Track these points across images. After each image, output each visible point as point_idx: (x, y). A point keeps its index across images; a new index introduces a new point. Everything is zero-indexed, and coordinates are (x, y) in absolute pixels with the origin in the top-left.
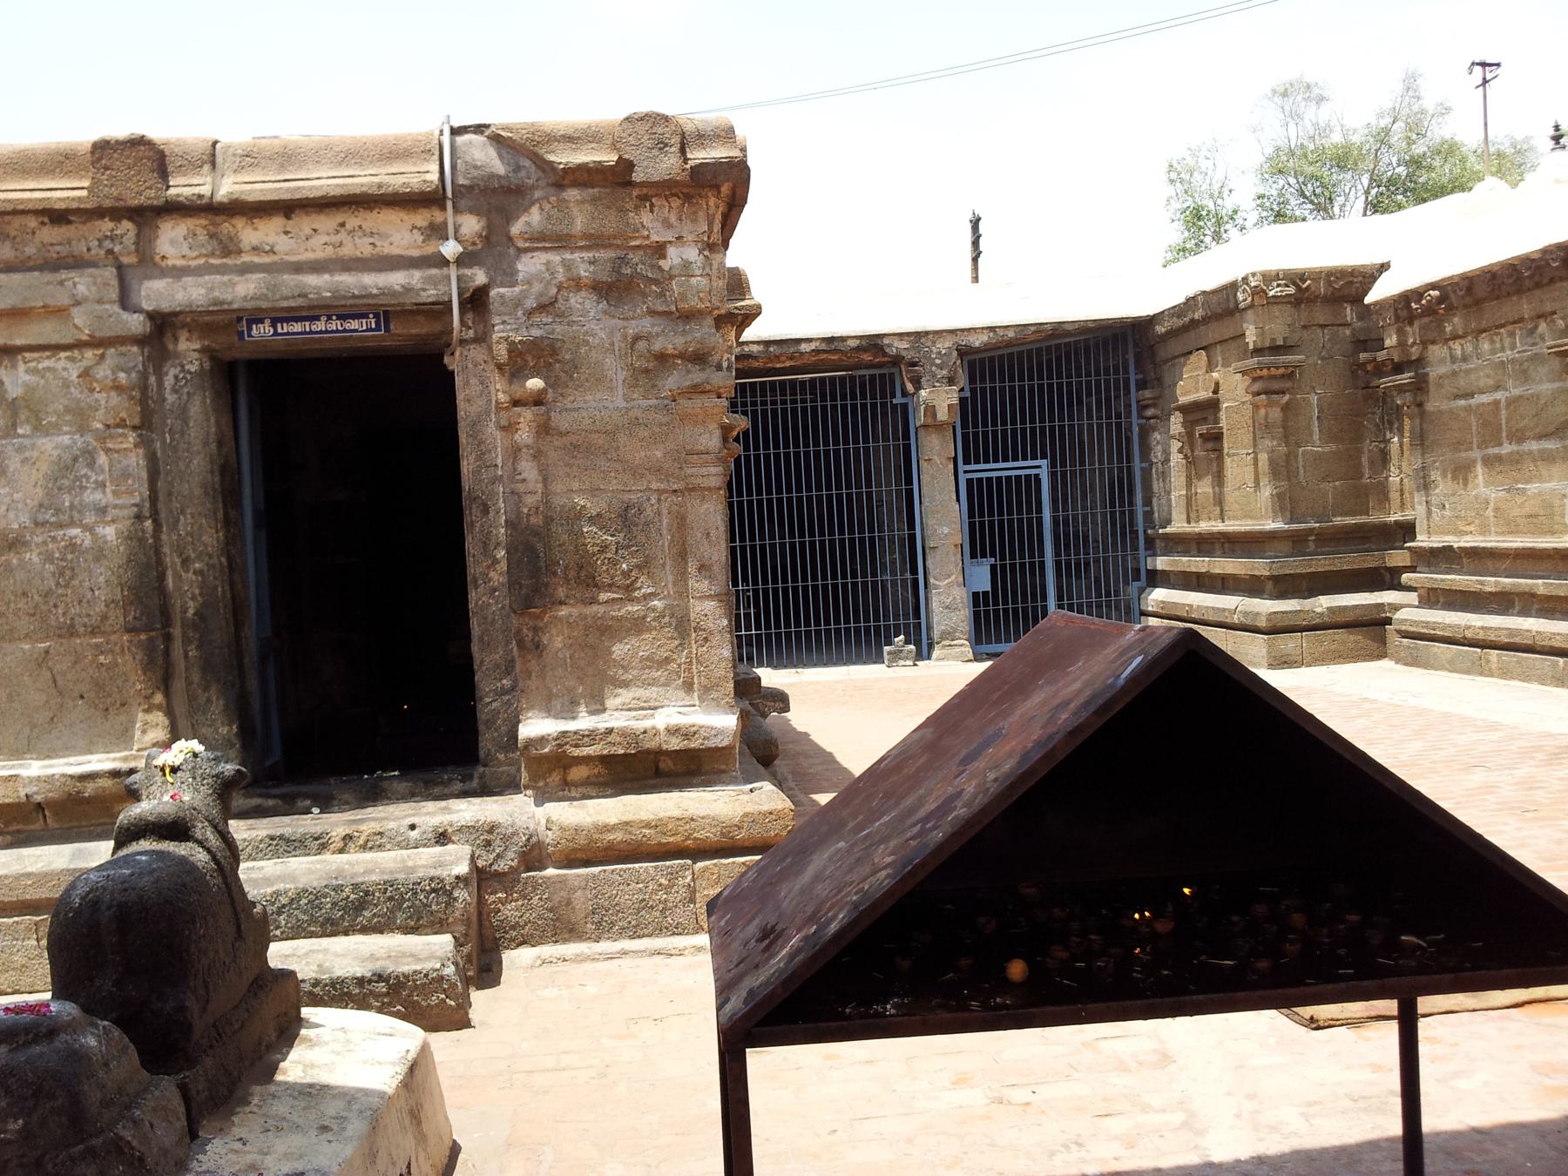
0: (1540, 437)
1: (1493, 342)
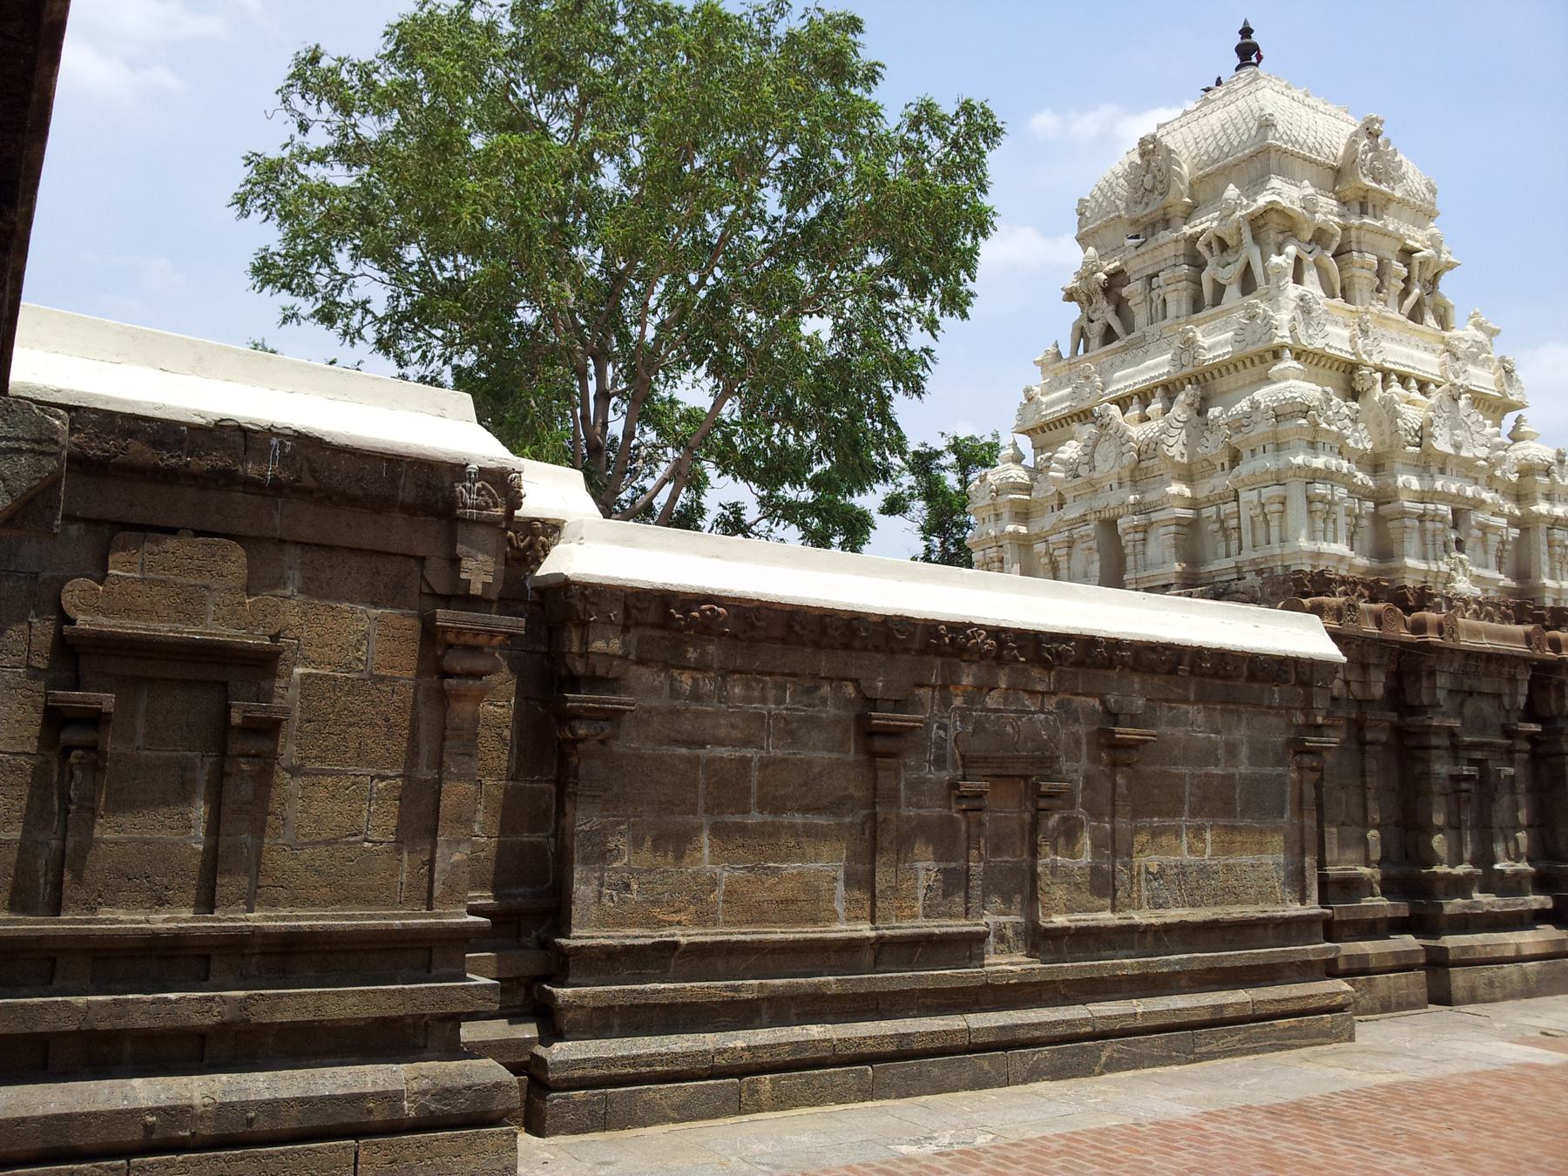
0: (805, 810)
1: (748, 687)
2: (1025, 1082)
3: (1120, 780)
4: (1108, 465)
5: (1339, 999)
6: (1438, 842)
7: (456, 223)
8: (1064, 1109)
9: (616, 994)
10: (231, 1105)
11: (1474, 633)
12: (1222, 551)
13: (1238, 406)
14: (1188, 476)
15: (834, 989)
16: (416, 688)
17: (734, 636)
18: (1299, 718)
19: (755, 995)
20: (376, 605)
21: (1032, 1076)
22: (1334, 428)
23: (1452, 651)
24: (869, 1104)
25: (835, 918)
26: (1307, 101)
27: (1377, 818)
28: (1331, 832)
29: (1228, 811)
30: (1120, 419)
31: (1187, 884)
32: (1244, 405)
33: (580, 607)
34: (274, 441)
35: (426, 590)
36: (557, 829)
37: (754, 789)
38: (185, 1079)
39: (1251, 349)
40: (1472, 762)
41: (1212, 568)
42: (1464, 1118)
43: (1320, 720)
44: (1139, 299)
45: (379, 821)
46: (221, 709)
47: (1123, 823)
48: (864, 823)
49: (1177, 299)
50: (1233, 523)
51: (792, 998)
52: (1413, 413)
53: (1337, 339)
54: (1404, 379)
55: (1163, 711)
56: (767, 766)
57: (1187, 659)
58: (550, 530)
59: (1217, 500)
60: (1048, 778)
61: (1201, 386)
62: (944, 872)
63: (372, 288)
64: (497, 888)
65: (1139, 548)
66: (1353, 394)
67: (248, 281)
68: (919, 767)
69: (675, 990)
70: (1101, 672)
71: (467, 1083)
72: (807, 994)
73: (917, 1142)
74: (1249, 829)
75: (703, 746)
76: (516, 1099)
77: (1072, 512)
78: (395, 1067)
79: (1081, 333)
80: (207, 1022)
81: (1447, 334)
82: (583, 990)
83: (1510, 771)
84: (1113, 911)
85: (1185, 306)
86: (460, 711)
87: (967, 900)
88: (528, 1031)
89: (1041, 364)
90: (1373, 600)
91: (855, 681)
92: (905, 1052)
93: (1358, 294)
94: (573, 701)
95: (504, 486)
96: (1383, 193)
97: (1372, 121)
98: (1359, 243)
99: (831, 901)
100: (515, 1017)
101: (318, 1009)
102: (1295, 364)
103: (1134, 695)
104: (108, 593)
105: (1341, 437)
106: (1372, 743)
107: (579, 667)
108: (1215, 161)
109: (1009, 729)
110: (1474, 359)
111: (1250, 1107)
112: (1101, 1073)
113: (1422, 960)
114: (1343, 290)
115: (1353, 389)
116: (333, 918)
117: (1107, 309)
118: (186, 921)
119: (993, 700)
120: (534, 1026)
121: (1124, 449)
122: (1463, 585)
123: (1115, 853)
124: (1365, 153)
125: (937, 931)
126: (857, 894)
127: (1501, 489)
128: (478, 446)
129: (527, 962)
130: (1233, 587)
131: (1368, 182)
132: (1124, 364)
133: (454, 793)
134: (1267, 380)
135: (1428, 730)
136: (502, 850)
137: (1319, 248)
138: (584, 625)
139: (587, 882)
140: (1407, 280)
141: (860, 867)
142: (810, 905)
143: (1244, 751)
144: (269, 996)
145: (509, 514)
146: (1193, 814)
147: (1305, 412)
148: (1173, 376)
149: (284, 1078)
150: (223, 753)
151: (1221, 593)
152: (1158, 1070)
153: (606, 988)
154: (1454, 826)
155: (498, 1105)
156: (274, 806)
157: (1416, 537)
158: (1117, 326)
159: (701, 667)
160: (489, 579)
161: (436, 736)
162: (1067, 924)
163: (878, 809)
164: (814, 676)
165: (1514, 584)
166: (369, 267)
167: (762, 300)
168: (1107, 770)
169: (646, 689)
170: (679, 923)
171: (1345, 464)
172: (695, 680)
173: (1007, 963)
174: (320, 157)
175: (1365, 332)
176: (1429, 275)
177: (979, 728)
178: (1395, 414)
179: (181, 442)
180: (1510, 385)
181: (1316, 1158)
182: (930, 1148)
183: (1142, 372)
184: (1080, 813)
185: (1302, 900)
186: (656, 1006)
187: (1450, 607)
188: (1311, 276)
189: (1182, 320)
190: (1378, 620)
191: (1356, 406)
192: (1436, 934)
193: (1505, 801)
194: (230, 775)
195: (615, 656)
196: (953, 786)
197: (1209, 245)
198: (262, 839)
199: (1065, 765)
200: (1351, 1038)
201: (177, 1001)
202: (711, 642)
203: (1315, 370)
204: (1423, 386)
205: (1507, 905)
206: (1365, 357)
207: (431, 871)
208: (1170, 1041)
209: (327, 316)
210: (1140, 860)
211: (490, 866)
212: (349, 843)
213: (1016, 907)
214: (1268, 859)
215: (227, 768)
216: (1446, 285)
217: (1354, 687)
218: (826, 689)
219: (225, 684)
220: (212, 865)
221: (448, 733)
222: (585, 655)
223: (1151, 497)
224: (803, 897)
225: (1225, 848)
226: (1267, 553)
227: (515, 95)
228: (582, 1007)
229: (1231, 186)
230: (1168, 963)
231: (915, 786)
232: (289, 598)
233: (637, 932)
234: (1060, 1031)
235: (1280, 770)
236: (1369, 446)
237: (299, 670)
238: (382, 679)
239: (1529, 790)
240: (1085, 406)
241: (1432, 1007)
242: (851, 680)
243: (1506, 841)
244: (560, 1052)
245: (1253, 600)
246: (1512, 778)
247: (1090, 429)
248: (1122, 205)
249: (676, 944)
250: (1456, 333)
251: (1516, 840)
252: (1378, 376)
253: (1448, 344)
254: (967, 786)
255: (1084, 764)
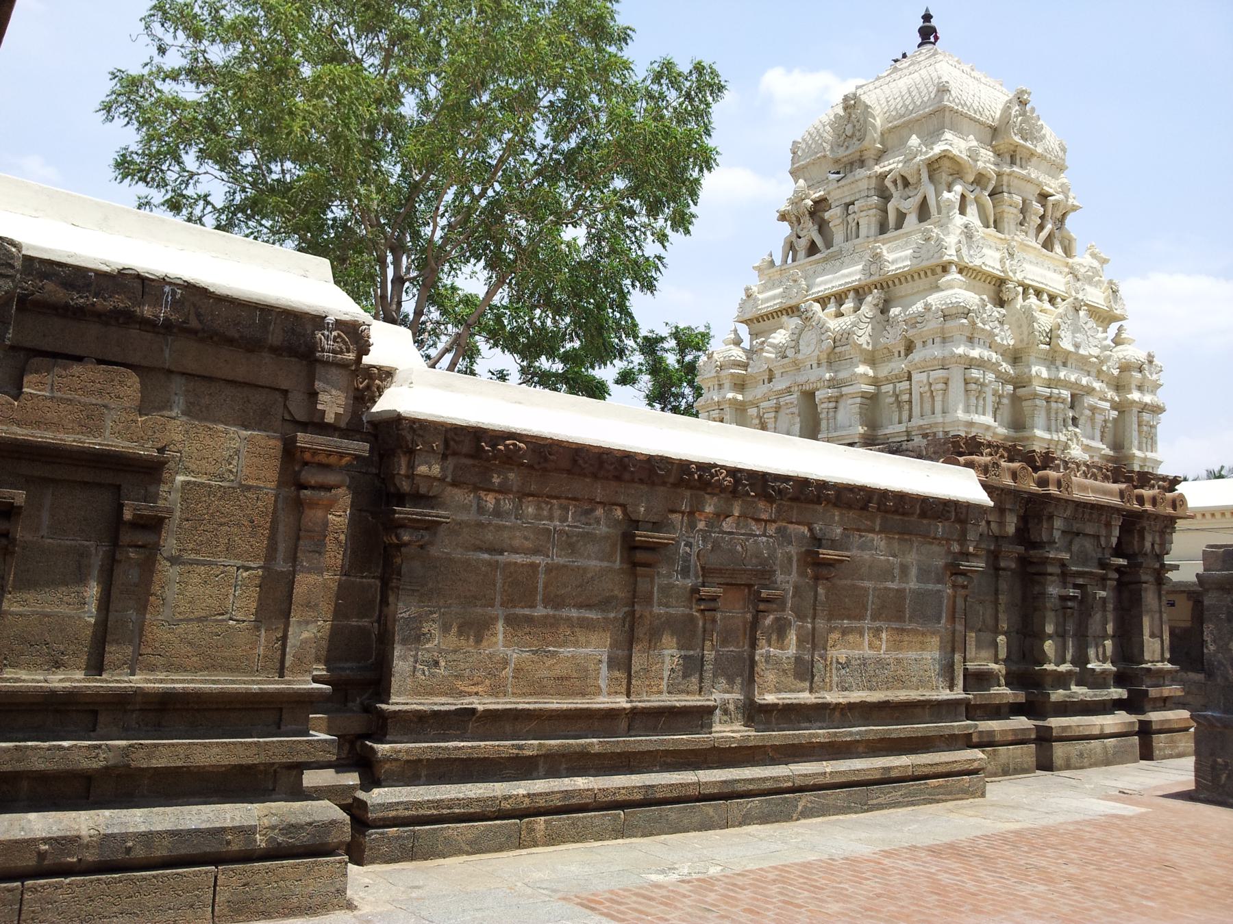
0: (580, 606)
1: (539, 508)
2: (740, 825)
3: (821, 590)
4: (810, 349)
5: (976, 765)
6: (1049, 646)
7: (288, 134)
8: (773, 847)
9: (424, 750)
10: (113, 836)
11: (1084, 488)
12: (896, 419)
13: (914, 308)
14: (872, 361)
15: (597, 749)
16: (277, 496)
17: (530, 467)
18: (956, 548)
19: (535, 753)
20: (246, 428)
21: (745, 820)
22: (987, 327)
23: (1067, 501)
24: (620, 841)
25: (598, 692)
26: (973, 74)
27: (1005, 626)
28: (972, 636)
29: (900, 619)
30: (820, 314)
31: (865, 671)
32: (919, 307)
33: (409, 438)
34: (167, 289)
35: (287, 417)
36: (380, 616)
37: (540, 589)
38: (74, 814)
39: (925, 264)
40: (1076, 586)
41: (887, 431)
42: (1074, 856)
43: (971, 549)
44: (838, 221)
45: (242, 603)
46: (116, 506)
47: (821, 624)
48: (624, 619)
49: (868, 223)
50: (906, 397)
51: (563, 755)
52: (1046, 318)
53: (990, 259)
54: (1038, 293)
55: (856, 539)
56: (551, 571)
57: (875, 498)
58: (387, 374)
59: (894, 379)
60: (766, 587)
61: (885, 291)
62: (684, 658)
63: (214, 185)
64: (329, 662)
65: (831, 414)
66: (1001, 303)
67: (112, 173)
68: (669, 576)
69: (470, 748)
70: (811, 506)
71: (308, 820)
72: (576, 753)
73: (663, 872)
74: (915, 632)
75: (501, 553)
76: (346, 834)
77: (780, 384)
78: (249, 806)
79: (791, 247)
80: (94, 766)
81: (1070, 261)
82: (399, 746)
83: (1103, 594)
84: (811, 692)
85: (874, 229)
86: (313, 516)
87: (701, 680)
88: (352, 779)
89: (759, 269)
90: (1011, 460)
91: (623, 506)
92: (650, 800)
93: (1006, 225)
94: (400, 513)
95: (356, 336)
96: (1028, 149)
97: (1023, 92)
98: (1009, 186)
99: (597, 679)
100: (340, 767)
101: (187, 757)
102: (959, 276)
103: (834, 525)
104: (21, 408)
105: (992, 335)
106: (1004, 569)
107: (405, 486)
108: (903, 116)
109: (739, 548)
110: (1089, 280)
111: (915, 847)
112: (798, 819)
113: (1033, 736)
114: (995, 221)
115: (1001, 299)
116: (201, 682)
117: (814, 228)
118: (79, 681)
119: (728, 525)
120: (356, 775)
121: (823, 337)
122: (1076, 452)
123: (814, 648)
124: (1016, 116)
125: (677, 704)
126: (617, 674)
127: (1106, 380)
128: (334, 302)
129: (354, 723)
130: (904, 447)
131: (1017, 139)
132: (824, 272)
133: (305, 583)
134: (937, 288)
135: (1045, 561)
136: (335, 633)
137: (979, 189)
138: (411, 452)
139: (404, 659)
140: (1042, 217)
141: (619, 652)
142: (579, 682)
143: (914, 572)
144: (147, 745)
145: (359, 359)
146: (873, 619)
147: (966, 314)
148: (863, 283)
149: (157, 814)
150: (115, 543)
151: (896, 449)
152: (841, 817)
153: (417, 745)
154: (1061, 635)
155: (333, 838)
156: (155, 588)
157: (1043, 414)
158: (819, 242)
159: (503, 490)
160: (341, 411)
161: (290, 538)
162: (776, 701)
163: (636, 607)
164: (591, 500)
165: (1111, 453)
166: (211, 167)
167: (534, 208)
168: (811, 583)
169: (458, 506)
170: (477, 694)
171: (994, 355)
172: (498, 501)
173: (728, 731)
174: (174, 76)
175: (1011, 255)
176: (1059, 215)
177: (716, 546)
178: (1032, 319)
179: (88, 285)
180: (1116, 302)
181: (971, 886)
182: (673, 877)
183: (838, 278)
184: (789, 615)
185: (951, 688)
186: (456, 759)
187: (1066, 468)
188: (972, 210)
189: (871, 239)
190: (1014, 476)
191: (1003, 311)
192: (1043, 717)
193: (1098, 617)
194: (120, 562)
195: (435, 478)
196: (695, 590)
197: (895, 182)
198: (144, 615)
199: (780, 577)
200: (983, 795)
201: (69, 748)
202: (512, 470)
203: (974, 282)
204: (1052, 299)
205: (1096, 695)
206: (1011, 274)
207: (284, 646)
208: (850, 795)
209: (174, 206)
210: (833, 653)
211: (324, 644)
212: (217, 621)
213: (737, 687)
214: (927, 655)
215: (118, 557)
216: (1069, 223)
217: (993, 525)
218: (600, 512)
219: (119, 487)
220: (102, 637)
221: (302, 534)
222: (411, 476)
223: (841, 375)
224: (575, 675)
225: (896, 645)
226: (932, 421)
227: (337, 34)
228: (396, 760)
229: (914, 137)
230: (851, 734)
231: (666, 590)
232: (174, 418)
233: (443, 700)
234: (768, 785)
235: (939, 586)
236: (1012, 343)
237: (180, 478)
238: (249, 488)
239: (1115, 609)
240: (793, 303)
241: (1039, 772)
242: (620, 505)
243: (1097, 647)
244: (378, 796)
245: (920, 457)
246: (1104, 600)
247: (794, 322)
248: (828, 148)
249: (474, 711)
250: (1076, 260)
251: (1104, 646)
252: (1020, 289)
253: (1072, 268)
254: (705, 591)
255: (794, 577)
